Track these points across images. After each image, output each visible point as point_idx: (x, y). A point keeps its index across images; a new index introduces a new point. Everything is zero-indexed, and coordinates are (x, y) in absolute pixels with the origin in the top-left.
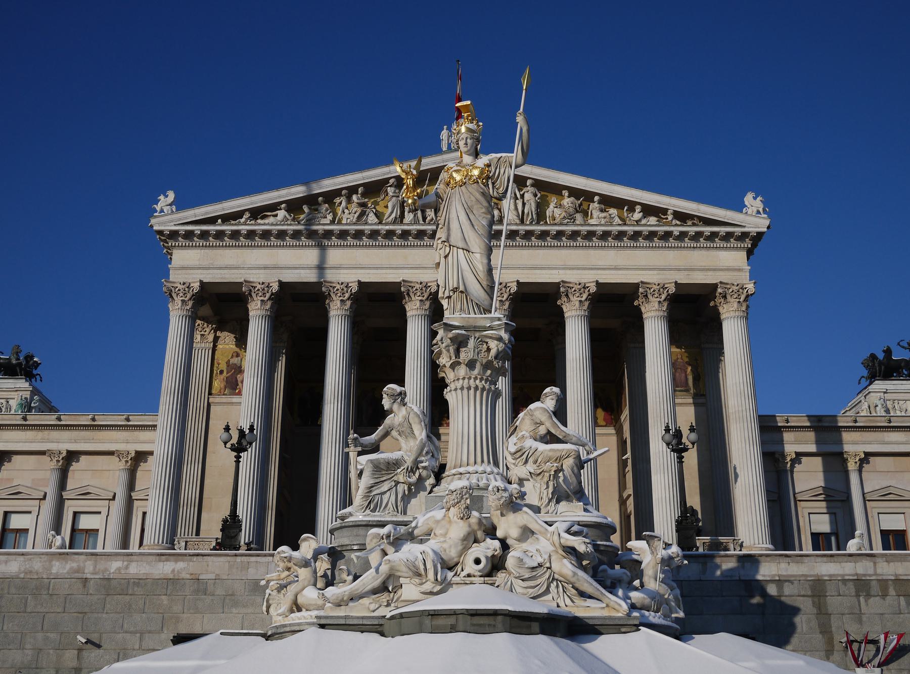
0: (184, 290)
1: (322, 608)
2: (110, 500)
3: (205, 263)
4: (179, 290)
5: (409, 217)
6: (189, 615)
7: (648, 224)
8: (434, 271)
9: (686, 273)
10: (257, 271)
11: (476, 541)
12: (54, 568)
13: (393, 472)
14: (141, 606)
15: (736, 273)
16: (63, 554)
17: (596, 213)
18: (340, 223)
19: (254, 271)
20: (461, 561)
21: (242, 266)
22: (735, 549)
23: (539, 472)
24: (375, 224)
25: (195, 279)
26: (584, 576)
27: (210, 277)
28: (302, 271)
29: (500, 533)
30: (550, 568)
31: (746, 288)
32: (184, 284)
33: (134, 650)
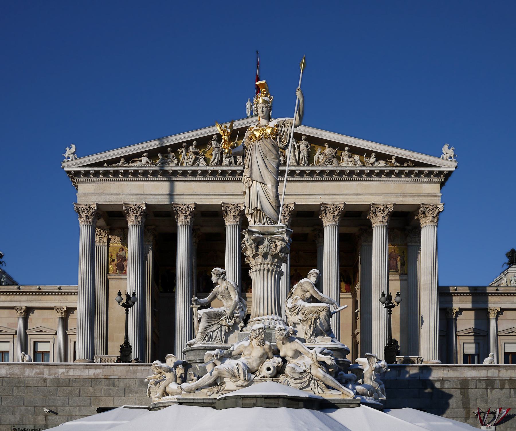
0: (87, 209)
1: (180, 394)
2: (54, 335)
3: (98, 192)
4: (84, 209)
5: (226, 161)
6: (105, 398)
7: (379, 165)
8: (242, 197)
9: (401, 198)
10: (131, 197)
11: (268, 358)
12: (26, 372)
13: (219, 319)
14: (78, 393)
15: (432, 198)
16: (31, 364)
17: (346, 159)
18: (182, 165)
19: (129, 197)
20: (259, 369)
21: (122, 194)
22: (418, 363)
23: (305, 319)
24: (204, 166)
25: (93, 202)
26: (330, 378)
27: (102, 201)
28: (160, 197)
29: (281, 354)
30: (310, 373)
31: (438, 208)
32: (86, 205)
33: (76, 415)
